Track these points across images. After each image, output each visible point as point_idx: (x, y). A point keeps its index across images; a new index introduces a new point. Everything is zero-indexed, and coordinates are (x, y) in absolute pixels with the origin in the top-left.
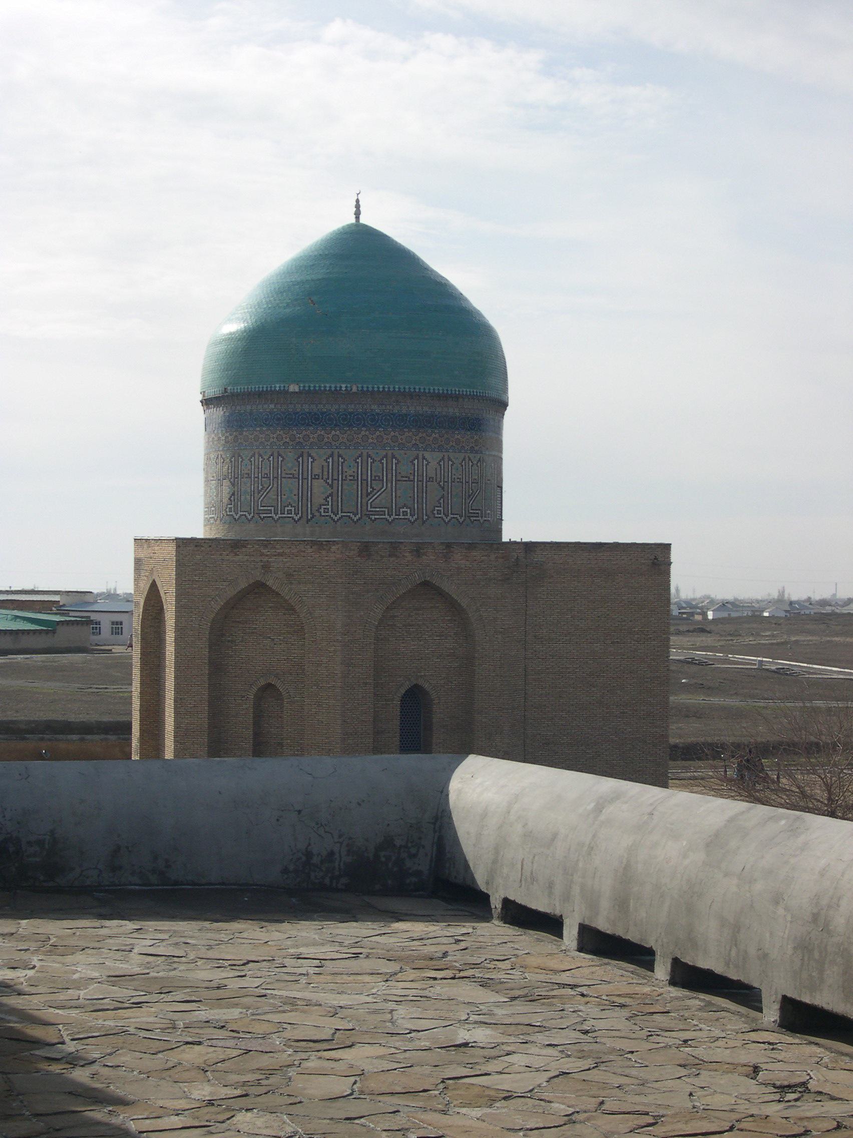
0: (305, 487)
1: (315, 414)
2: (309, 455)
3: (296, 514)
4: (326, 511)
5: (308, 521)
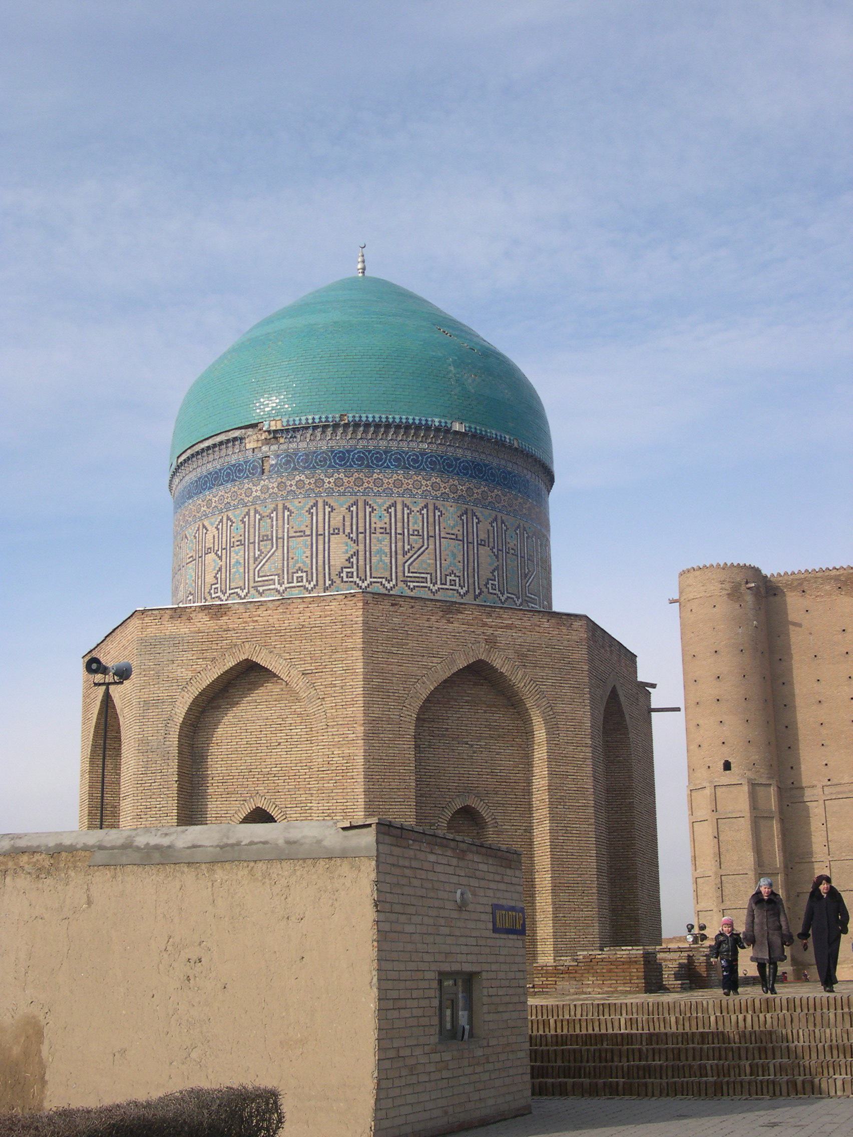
1: (478, 465)
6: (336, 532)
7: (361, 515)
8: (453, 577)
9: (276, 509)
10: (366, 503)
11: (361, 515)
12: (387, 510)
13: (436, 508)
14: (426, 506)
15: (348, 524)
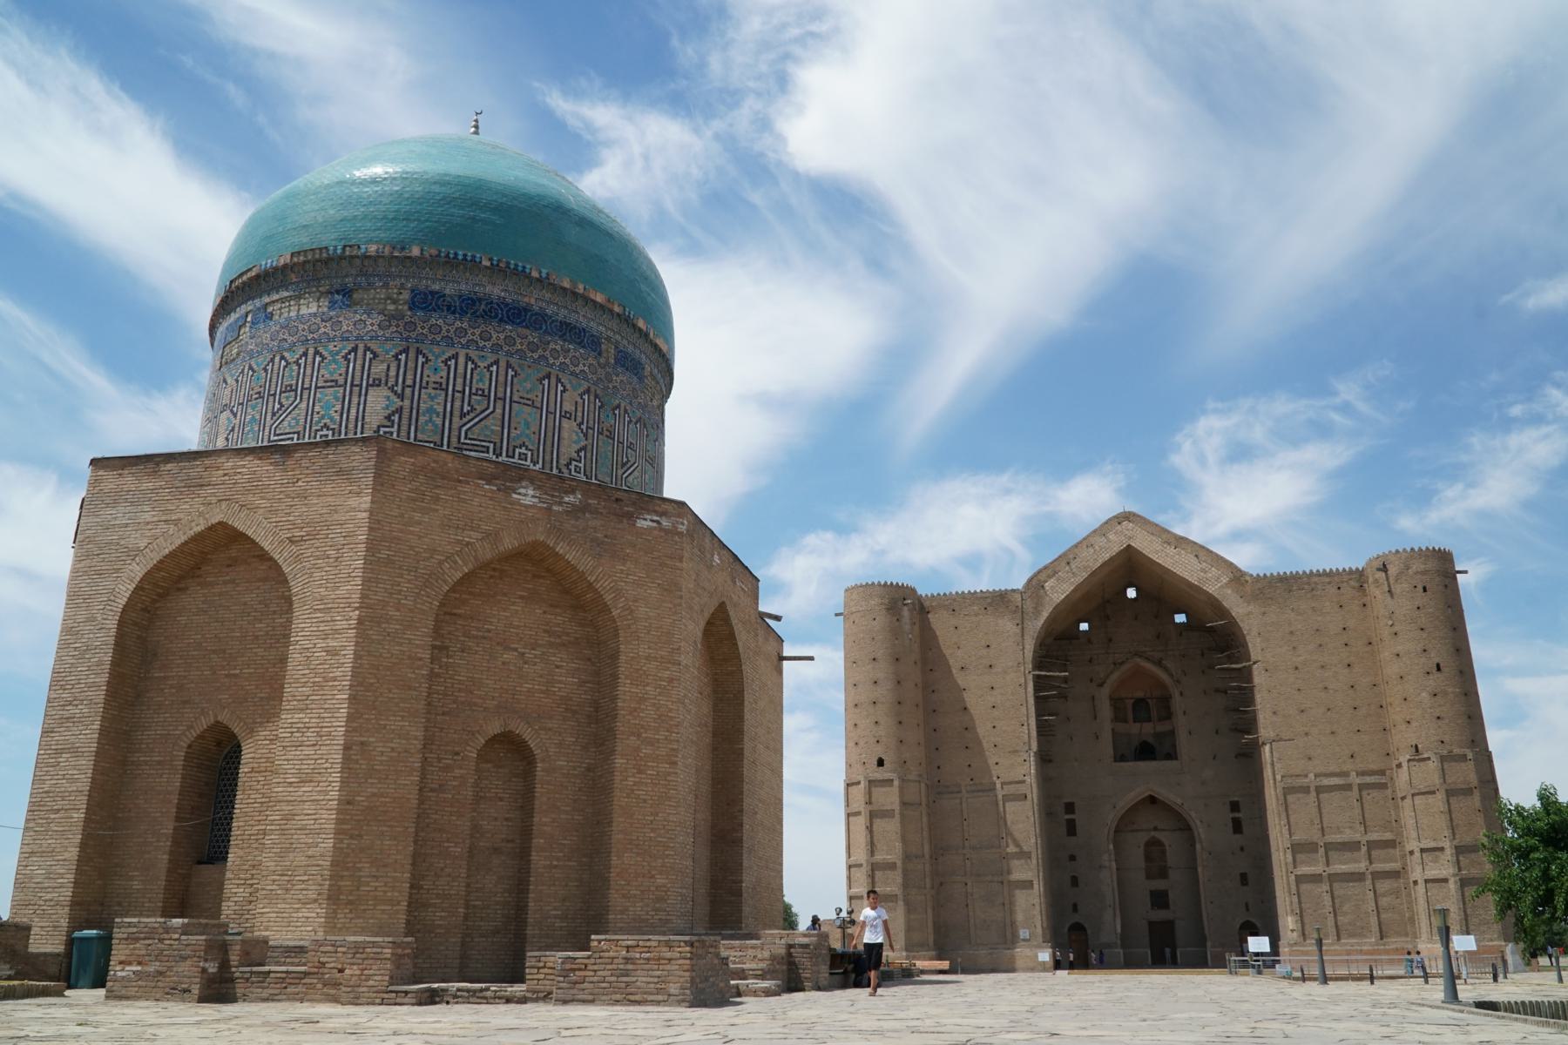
0: (551, 424)
2: (558, 380)
4: (578, 470)
6: (377, 383)
7: (411, 364)
8: (523, 450)
9: (305, 354)
10: (419, 352)
11: (411, 364)
12: (445, 362)
13: (509, 366)
14: (497, 362)
15: (392, 373)
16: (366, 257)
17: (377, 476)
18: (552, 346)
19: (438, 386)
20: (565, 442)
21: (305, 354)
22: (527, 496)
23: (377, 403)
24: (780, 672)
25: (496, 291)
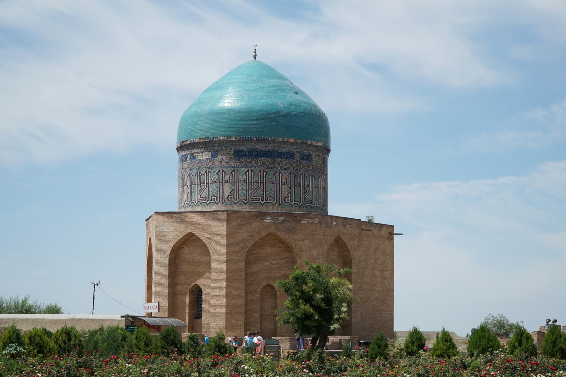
2: (280, 172)
3: (274, 201)
4: (288, 200)
5: (280, 205)
6: (226, 182)
7: (236, 175)
9: (206, 172)
10: (237, 171)
11: (236, 175)
12: (245, 173)
13: (264, 171)
14: (260, 171)
15: (231, 178)
16: (219, 141)
17: (227, 221)
18: (277, 161)
19: (244, 181)
20: (283, 192)
21: (206, 172)
22: (268, 220)
23: (227, 188)
24: (393, 239)
25: (259, 147)
